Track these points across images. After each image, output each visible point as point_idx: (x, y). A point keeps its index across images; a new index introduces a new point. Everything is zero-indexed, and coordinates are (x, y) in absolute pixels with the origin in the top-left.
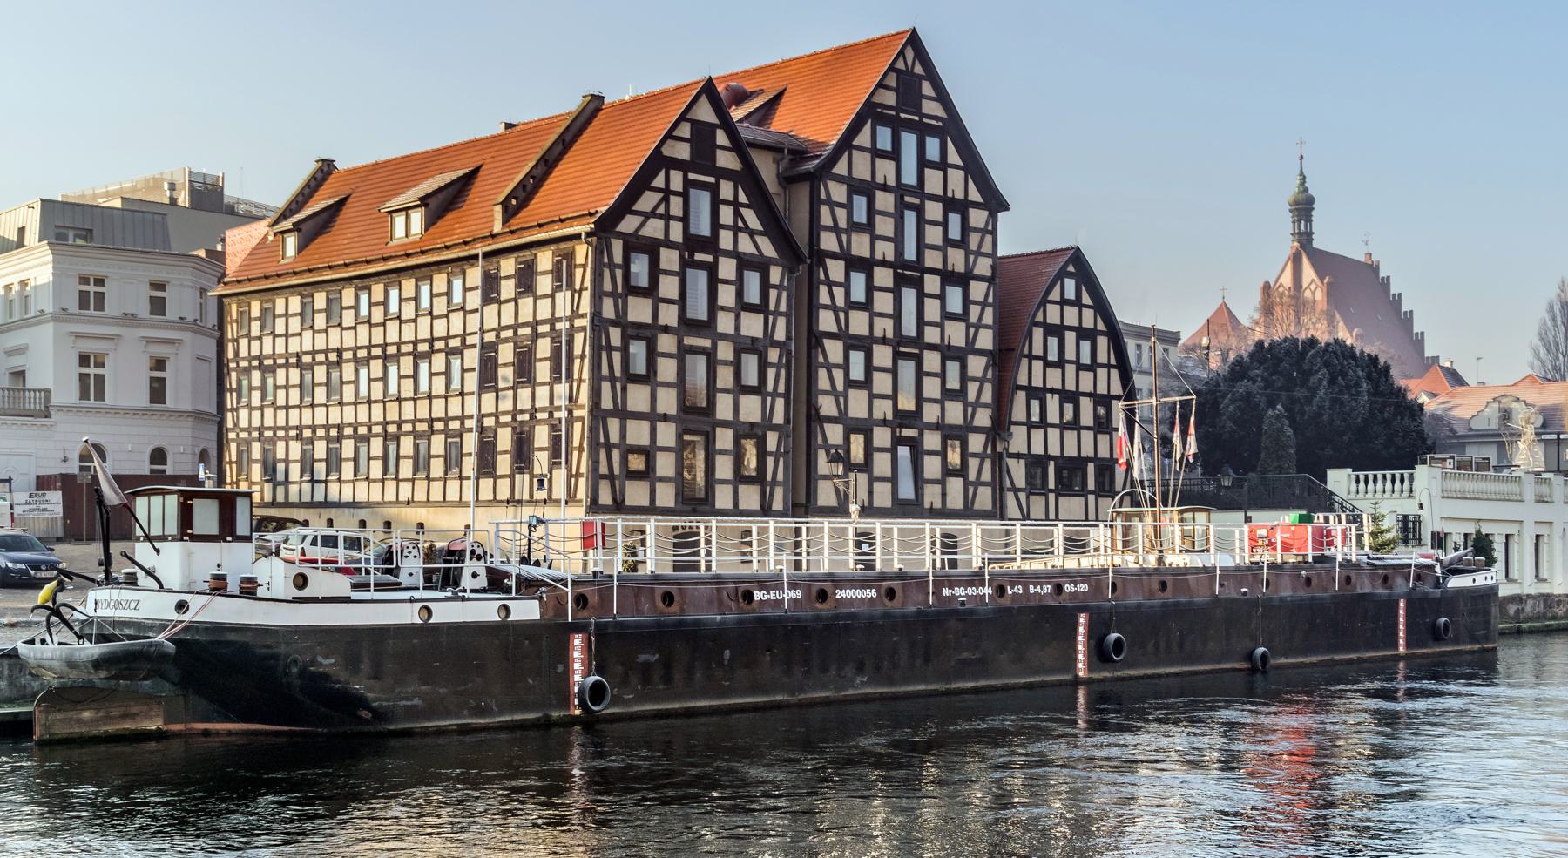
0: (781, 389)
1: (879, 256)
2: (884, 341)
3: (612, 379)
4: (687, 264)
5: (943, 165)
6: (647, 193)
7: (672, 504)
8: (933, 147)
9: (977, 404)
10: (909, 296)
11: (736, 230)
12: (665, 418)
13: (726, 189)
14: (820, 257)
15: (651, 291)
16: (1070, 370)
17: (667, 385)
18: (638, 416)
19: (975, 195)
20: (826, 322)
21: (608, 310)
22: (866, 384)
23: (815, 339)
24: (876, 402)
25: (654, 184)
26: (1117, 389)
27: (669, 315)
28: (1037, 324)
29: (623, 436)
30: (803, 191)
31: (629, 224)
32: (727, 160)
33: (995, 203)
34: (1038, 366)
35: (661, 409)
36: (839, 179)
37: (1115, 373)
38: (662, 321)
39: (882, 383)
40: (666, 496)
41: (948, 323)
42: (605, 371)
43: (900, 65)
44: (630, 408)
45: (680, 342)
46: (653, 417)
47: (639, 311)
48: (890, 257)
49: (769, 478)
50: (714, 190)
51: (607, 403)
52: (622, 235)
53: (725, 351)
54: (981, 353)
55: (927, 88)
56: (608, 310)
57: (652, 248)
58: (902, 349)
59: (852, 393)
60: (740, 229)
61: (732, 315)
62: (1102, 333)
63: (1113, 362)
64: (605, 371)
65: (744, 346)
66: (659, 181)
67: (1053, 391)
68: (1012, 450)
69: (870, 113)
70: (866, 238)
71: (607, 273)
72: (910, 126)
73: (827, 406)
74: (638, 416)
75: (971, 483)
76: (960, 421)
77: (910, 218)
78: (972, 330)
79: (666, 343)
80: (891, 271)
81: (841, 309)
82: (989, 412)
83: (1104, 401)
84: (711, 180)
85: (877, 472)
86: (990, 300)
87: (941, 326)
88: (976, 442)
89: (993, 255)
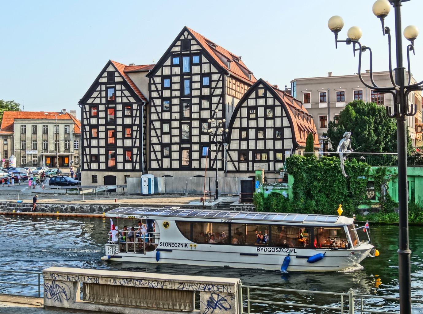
0: (138, 137)
1: (173, 95)
2: (176, 120)
3: (87, 139)
4: (106, 109)
5: (200, 64)
6: (95, 92)
7: (105, 168)
8: (196, 59)
11: (121, 97)
12: (102, 147)
13: (118, 87)
14: (152, 99)
15: (97, 116)
19: (214, 70)
20: (154, 117)
21: (85, 122)
22: (169, 133)
24: (173, 138)
25: (97, 90)
27: (102, 122)
31: (90, 101)
34: (245, 121)
38: (100, 123)
40: (103, 166)
41: (201, 111)
43: (182, 38)
45: (106, 128)
46: (98, 147)
47: (94, 121)
49: (134, 161)
50: (115, 87)
51: (85, 144)
52: (88, 104)
53: (120, 128)
55: (193, 42)
56: (85, 122)
57: (96, 106)
58: (182, 121)
59: (163, 136)
60: (123, 97)
61: (121, 119)
63: (284, 114)
64: (85, 137)
65: (125, 126)
66: (98, 89)
67: (252, 128)
69: (169, 54)
71: (84, 114)
73: (155, 140)
77: (187, 83)
79: (102, 128)
80: (179, 99)
81: (159, 113)
84: (114, 85)
86: (221, 101)
87: (199, 112)
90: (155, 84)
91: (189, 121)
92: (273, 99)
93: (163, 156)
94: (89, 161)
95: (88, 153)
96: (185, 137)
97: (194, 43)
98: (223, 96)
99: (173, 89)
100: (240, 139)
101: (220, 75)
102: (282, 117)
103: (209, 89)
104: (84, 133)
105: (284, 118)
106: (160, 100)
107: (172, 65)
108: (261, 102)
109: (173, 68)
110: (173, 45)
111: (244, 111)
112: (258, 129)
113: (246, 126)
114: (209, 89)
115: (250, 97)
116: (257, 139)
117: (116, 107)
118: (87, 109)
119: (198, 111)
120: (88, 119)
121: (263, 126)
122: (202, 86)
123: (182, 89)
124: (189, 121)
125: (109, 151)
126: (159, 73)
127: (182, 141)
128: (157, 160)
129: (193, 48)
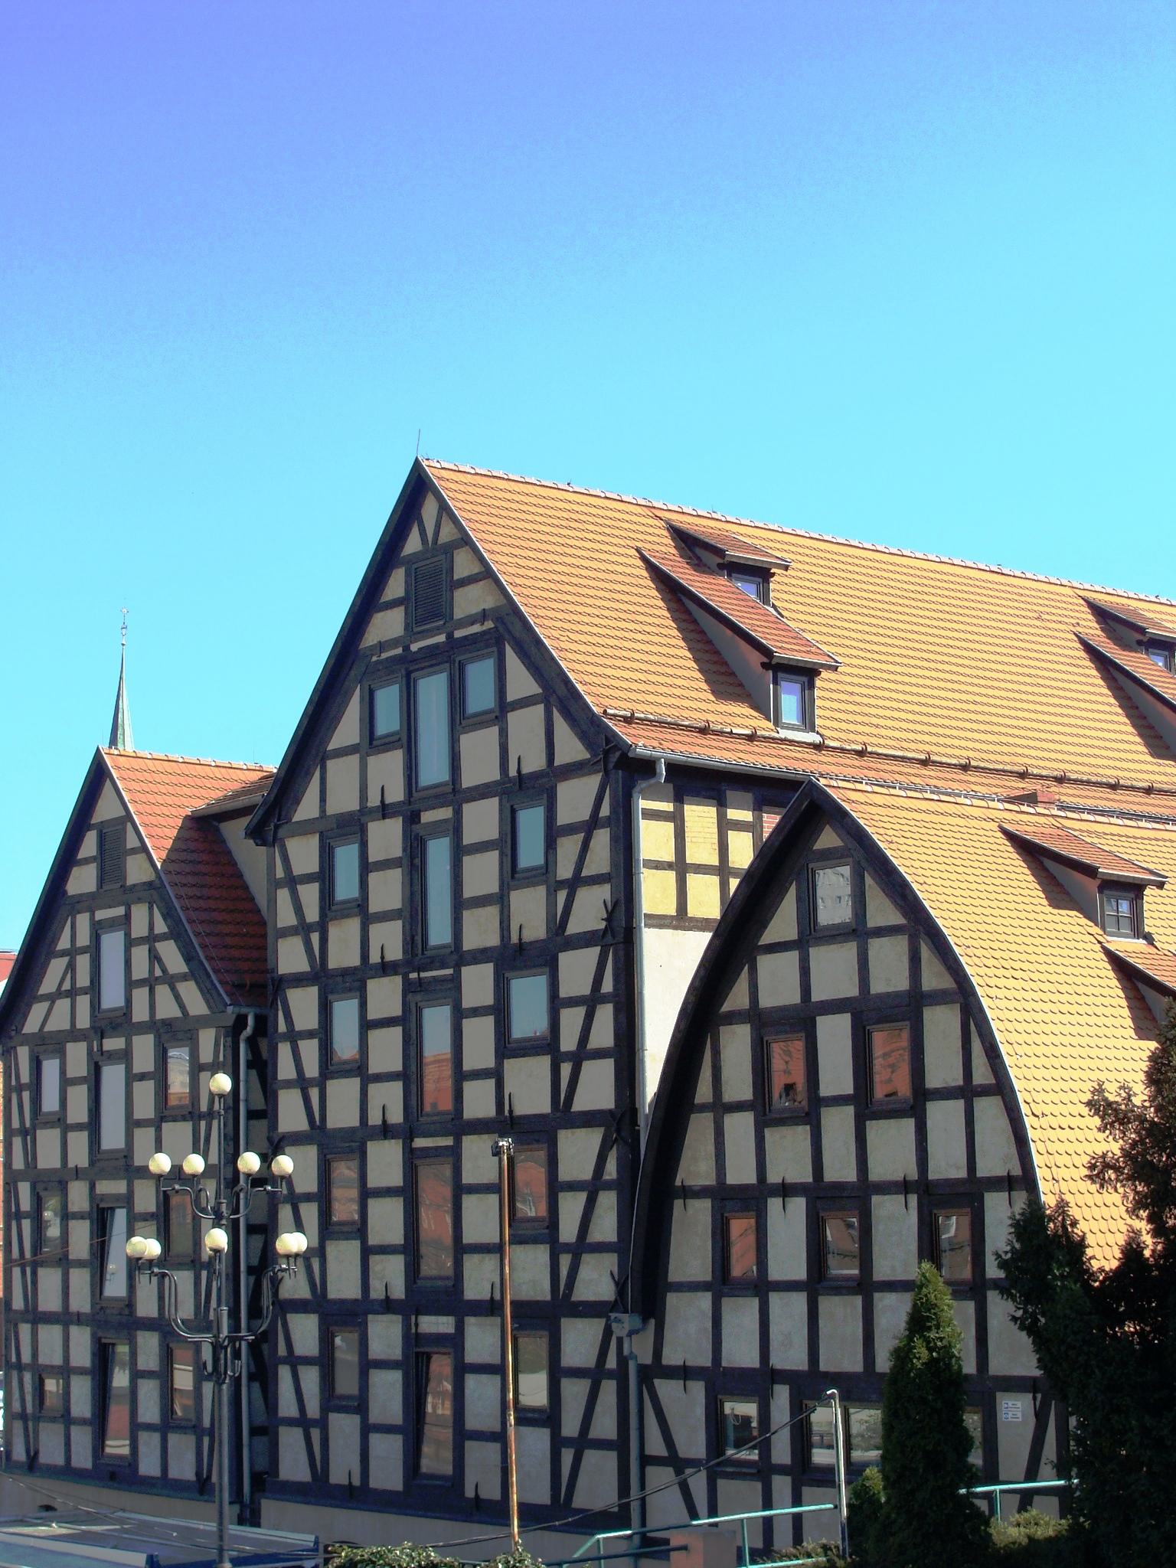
9: (582, 1246)
10: (436, 1021)
11: (151, 983)
12: (79, 1319)
13: (140, 919)
16: (838, 1123)
17: (80, 1264)
18: (49, 1318)
19: (570, 748)
28: (733, 1018)
29: (35, 1354)
34: (740, 1127)
35: (74, 1306)
36: (305, 829)
41: (509, 1065)
44: (42, 1308)
46: (66, 1318)
48: (395, 953)
52: (27, 1039)
54: (589, 1119)
55: (463, 565)
58: (420, 1143)
61: (151, 1131)
62: (939, 998)
63: (982, 1075)
67: (786, 1190)
68: (672, 1357)
70: (354, 925)
72: (433, 658)
74: (49, 1318)
75: (569, 1442)
76: (542, 1291)
77: (438, 852)
78: (566, 1069)
79: (78, 1196)
80: (398, 980)
82: (610, 1261)
84: (120, 911)
85: (375, 1416)
86: (608, 986)
87: (497, 1075)
88: (580, 1341)
90: (292, 882)
91: (448, 1141)
92: (901, 943)
93: (331, 1401)
94: (29, 1409)
95: (26, 1358)
96: (436, 1264)
97: (466, 574)
98: (620, 938)
99: (373, 908)
100: (722, 1283)
101: (593, 782)
102: (967, 1092)
103: (541, 892)
104: (14, 1224)
105: (982, 1105)
106: (313, 992)
107: (372, 743)
109: (373, 761)
110: (368, 600)
111: (735, 1045)
112: (823, 1198)
113: (752, 1179)
114: (541, 892)
115: (768, 937)
116: (817, 1282)
118: (25, 1078)
119: (490, 1063)
120: (27, 1134)
121: (850, 1175)
122: (512, 875)
123: (415, 913)
124: (448, 1141)
126: (307, 808)
127: (421, 1296)
128: (302, 1422)
129: (469, 601)
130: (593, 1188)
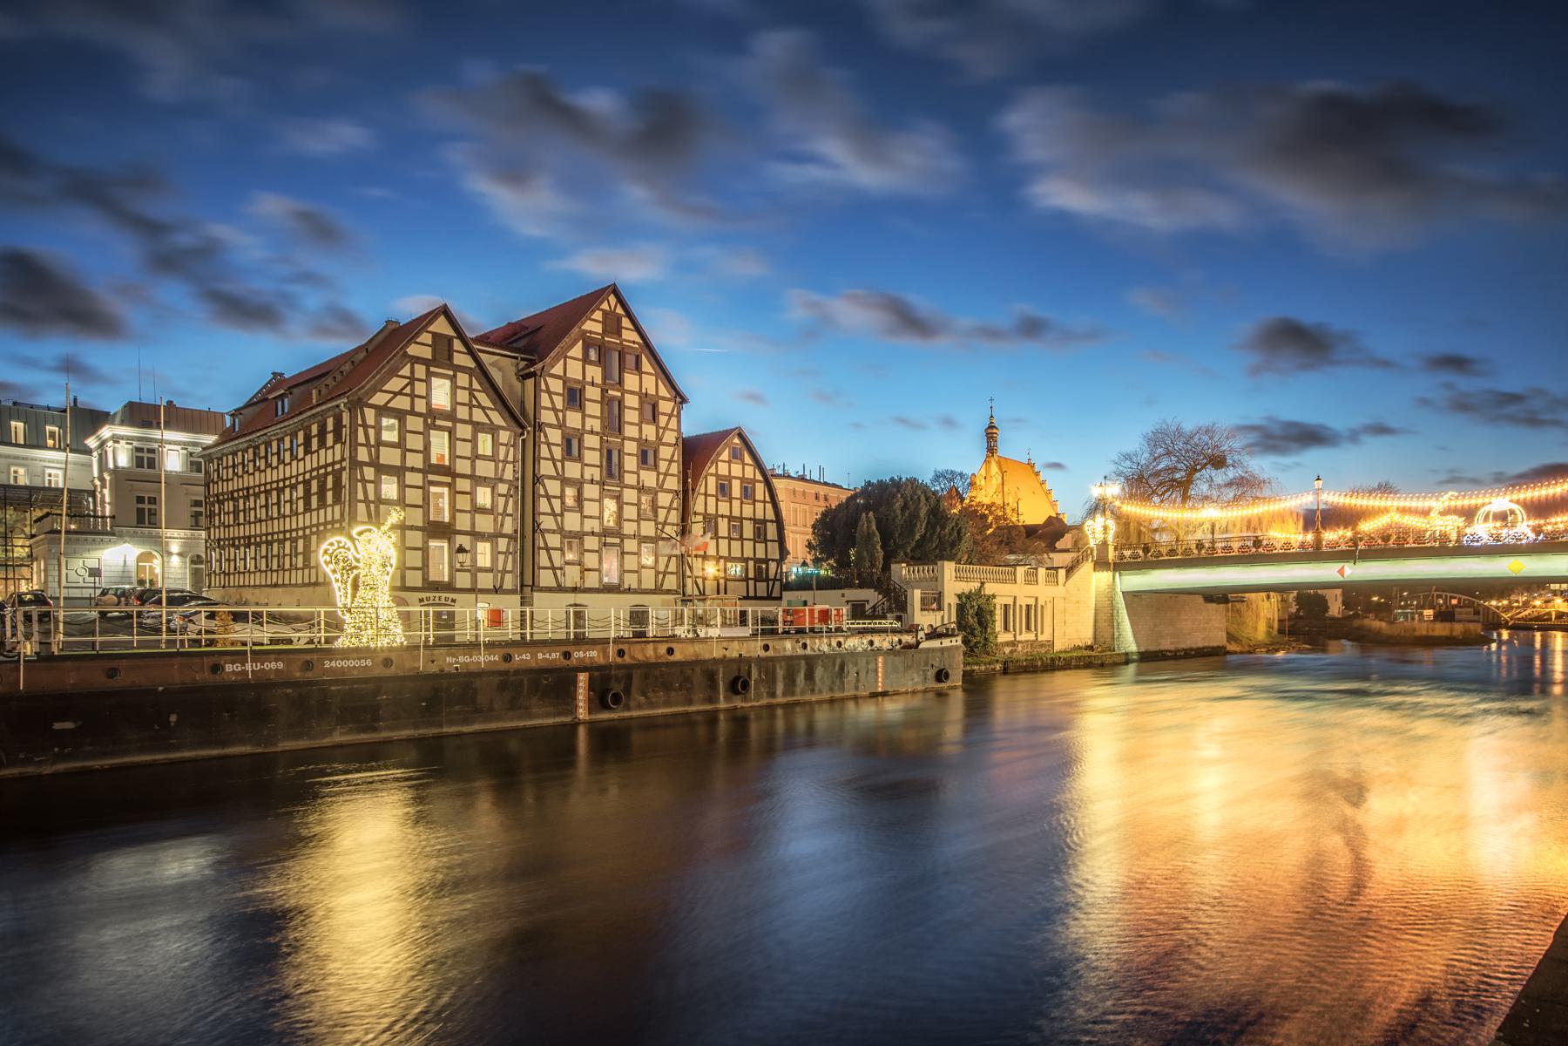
3: (366, 501)
11: (471, 407)
13: (463, 379)
19: (663, 392)
23: (537, 479)
26: (770, 515)
30: (530, 383)
32: (462, 359)
33: (680, 398)
34: (711, 500)
37: (769, 506)
38: (409, 464)
39: (591, 508)
42: (360, 496)
64: (360, 496)
66: (406, 371)
73: (547, 522)
83: (759, 525)
89: (679, 430)
108: (736, 469)
117: (455, 427)
125: (446, 545)
130: (669, 509)
